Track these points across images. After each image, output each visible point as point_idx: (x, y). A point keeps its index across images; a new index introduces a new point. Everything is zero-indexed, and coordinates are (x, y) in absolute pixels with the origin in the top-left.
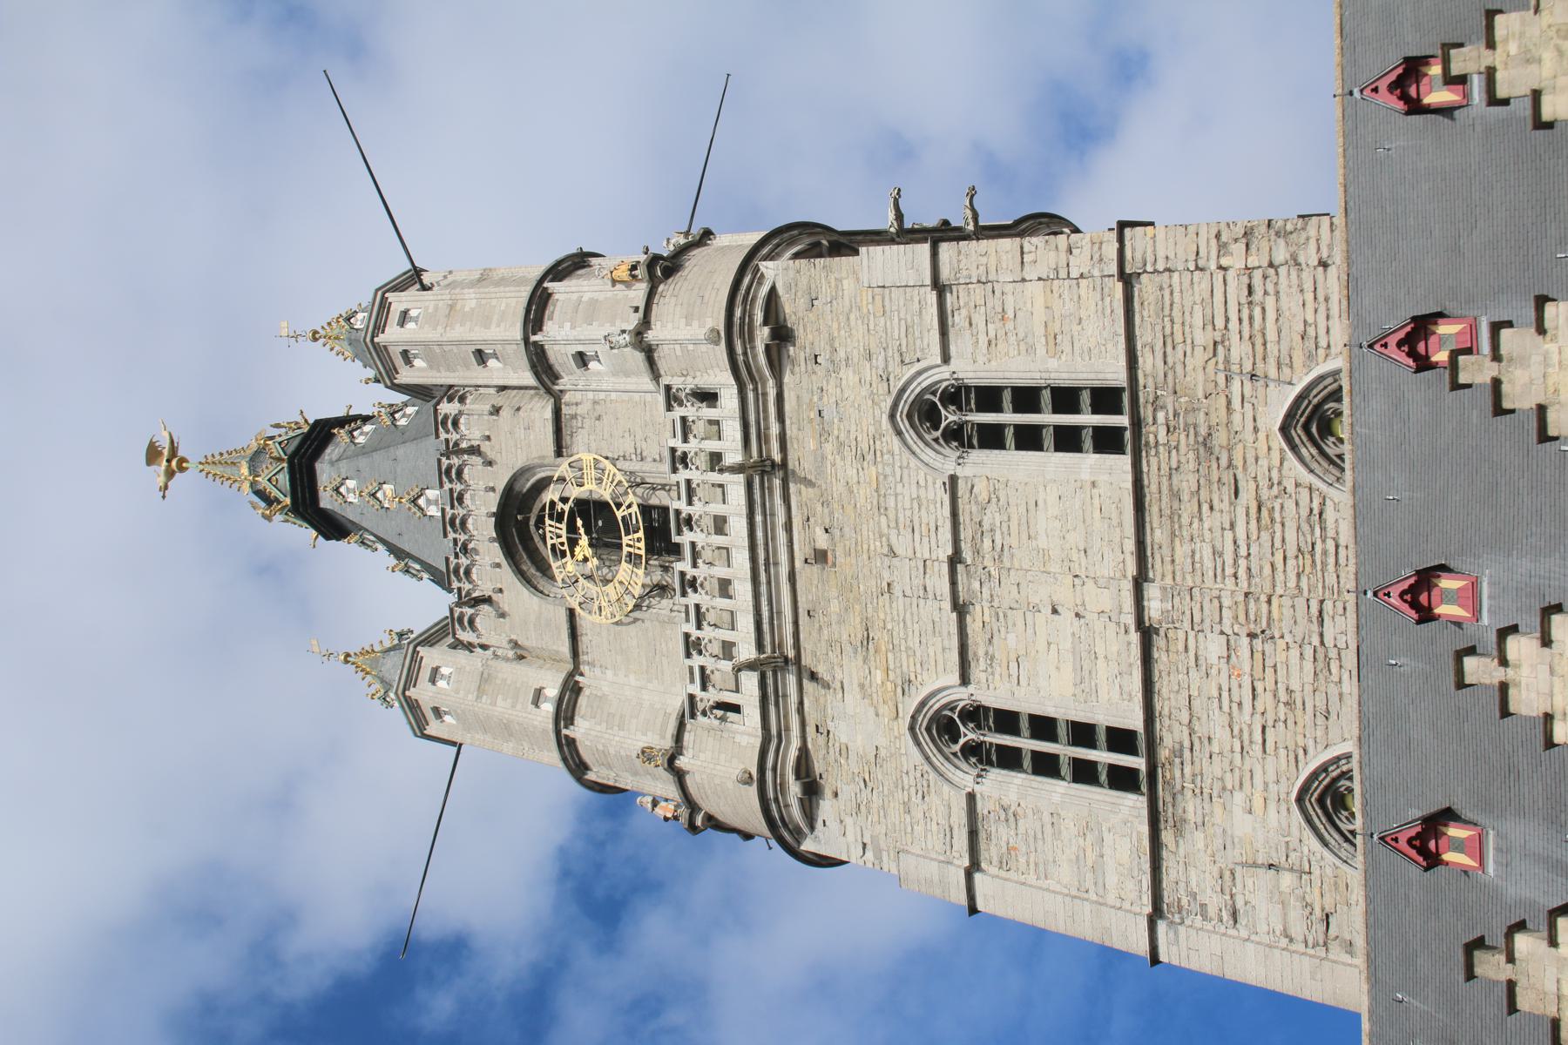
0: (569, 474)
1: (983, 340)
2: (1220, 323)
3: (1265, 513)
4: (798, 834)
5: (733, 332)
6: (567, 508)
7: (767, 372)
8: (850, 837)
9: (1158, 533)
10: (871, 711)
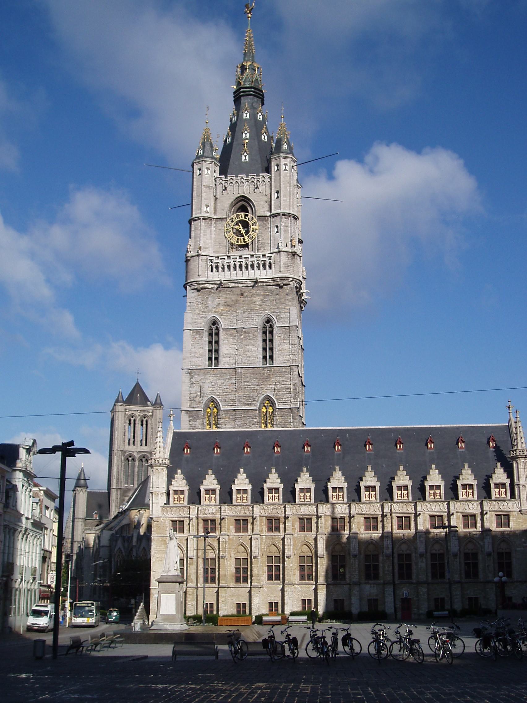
0: (253, 221)
1: (280, 335)
2: (283, 383)
3: (254, 391)
4: (190, 287)
5: (282, 279)
6: (247, 220)
7: (275, 283)
8: (191, 299)
9: (250, 371)
10: (215, 306)
